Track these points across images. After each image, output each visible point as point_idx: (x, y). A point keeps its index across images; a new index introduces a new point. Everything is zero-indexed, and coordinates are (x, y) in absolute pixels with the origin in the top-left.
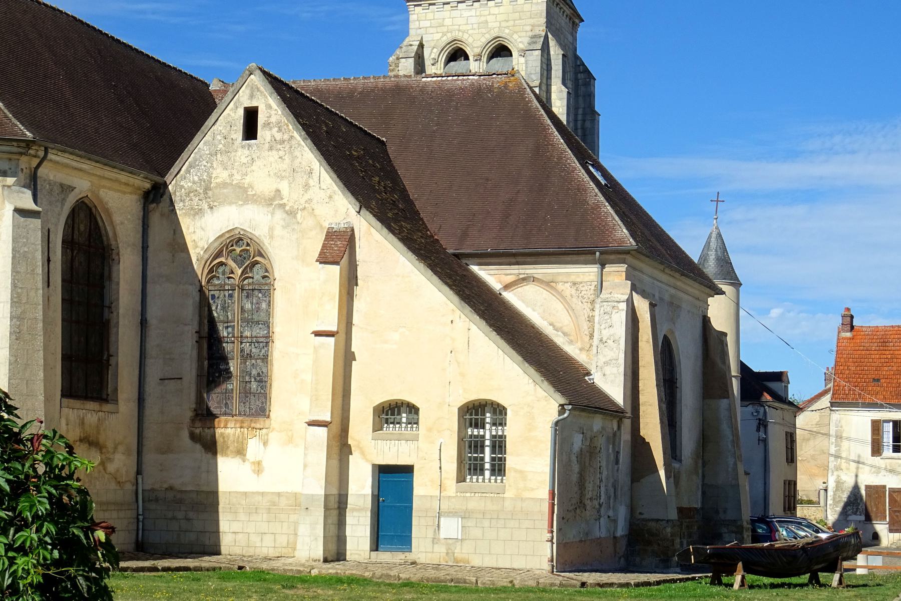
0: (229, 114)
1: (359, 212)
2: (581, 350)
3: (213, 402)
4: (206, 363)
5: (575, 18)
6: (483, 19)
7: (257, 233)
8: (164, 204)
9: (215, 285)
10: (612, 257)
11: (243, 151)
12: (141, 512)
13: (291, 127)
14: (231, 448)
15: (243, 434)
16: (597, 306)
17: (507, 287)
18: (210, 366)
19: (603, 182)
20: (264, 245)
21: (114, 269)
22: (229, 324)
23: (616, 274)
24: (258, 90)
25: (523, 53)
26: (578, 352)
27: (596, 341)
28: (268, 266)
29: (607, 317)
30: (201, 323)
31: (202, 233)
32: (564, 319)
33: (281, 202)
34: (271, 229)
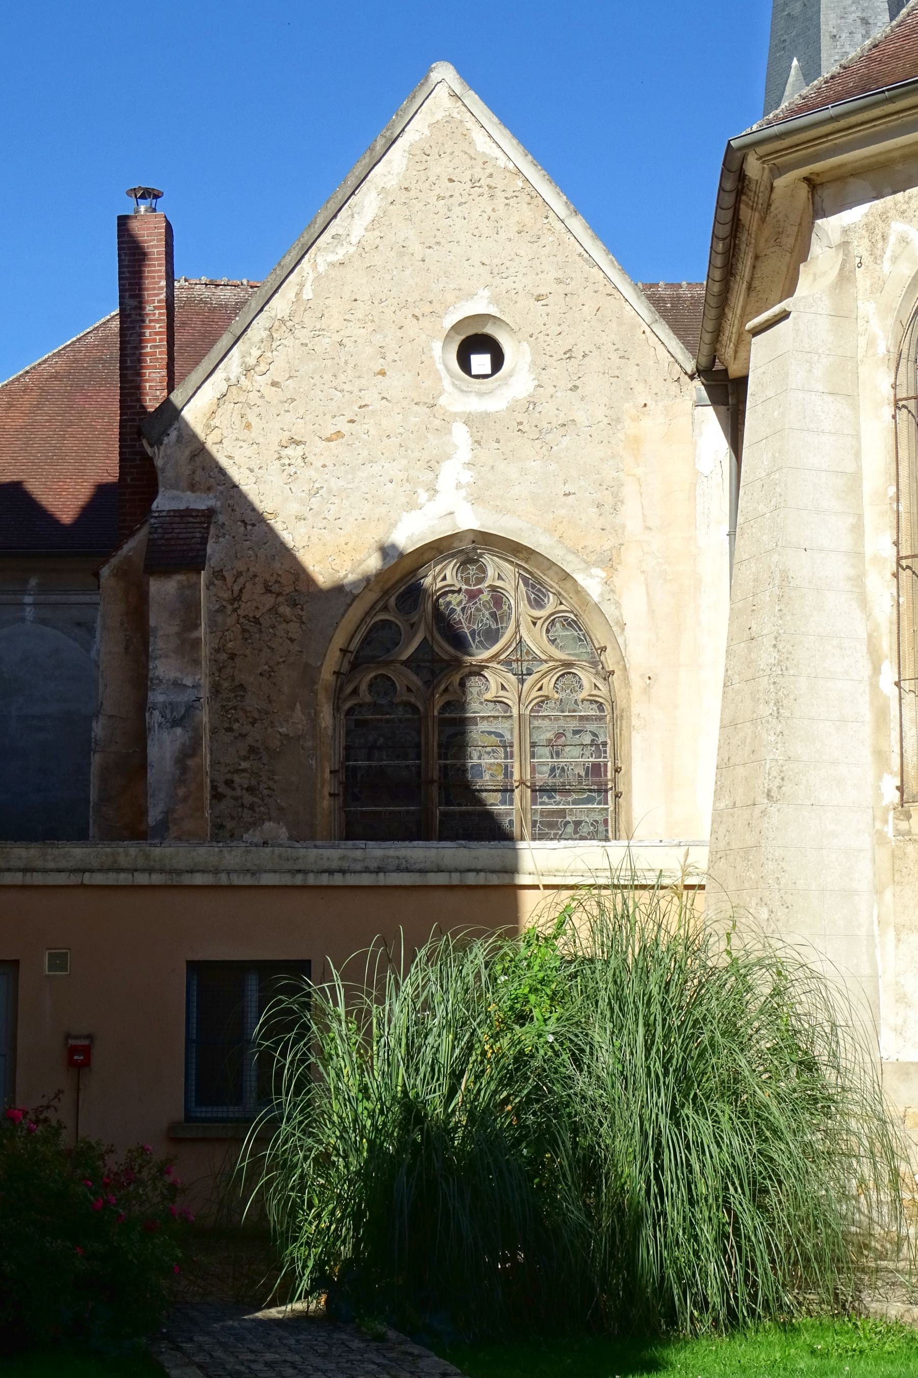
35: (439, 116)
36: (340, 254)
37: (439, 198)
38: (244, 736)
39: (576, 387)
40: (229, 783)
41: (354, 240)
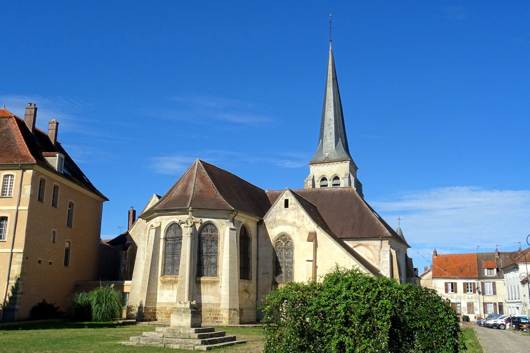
1: (317, 227)
2: (377, 264)
3: (277, 280)
4: (275, 269)
5: (356, 168)
6: (331, 169)
7: (289, 233)
8: (263, 225)
9: (277, 247)
10: (384, 238)
11: (285, 211)
12: (258, 311)
13: (298, 204)
16: (381, 252)
17: (354, 247)
18: (276, 270)
19: (378, 217)
21: (251, 243)
23: (386, 243)
24: (288, 194)
25: (343, 179)
26: (376, 265)
27: (381, 262)
28: (292, 242)
29: (384, 255)
30: (274, 258)
31: (274, 233)
32: (371, 255)
33: (296, 225)
34: (293, 232)
35: (154, 199)
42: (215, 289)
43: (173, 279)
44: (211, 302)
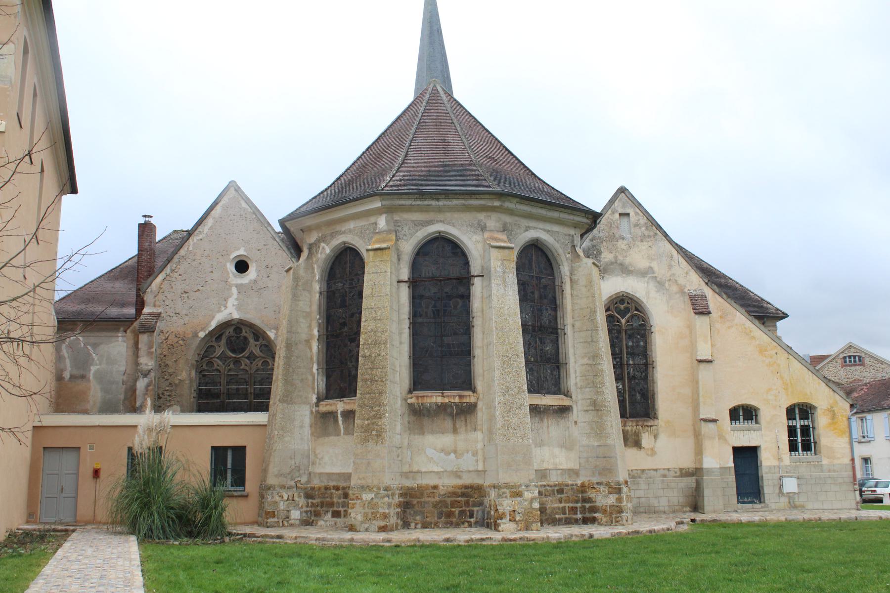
0: (608, 217)
7: (638, 296)
14: (630, 440)
15: (638, 430)
20: (643, 303)
22: (617, 356)
33: (653, 275)
34: (648, 293)
36: (201, 237)
37: (231, 220)
38: (167, 380)
39: (268, 277)
40: (163, 394)
41: (205, 232)
42: (565, 431)
43: (453, 401)
44: (558, 467)
